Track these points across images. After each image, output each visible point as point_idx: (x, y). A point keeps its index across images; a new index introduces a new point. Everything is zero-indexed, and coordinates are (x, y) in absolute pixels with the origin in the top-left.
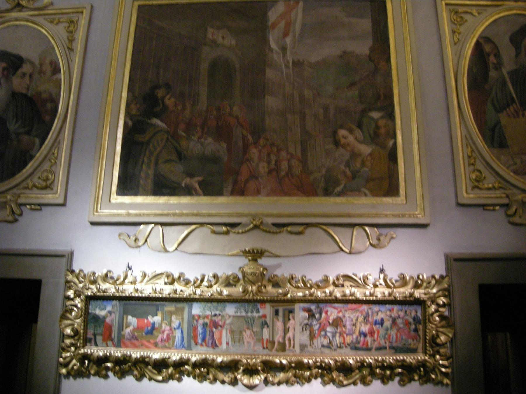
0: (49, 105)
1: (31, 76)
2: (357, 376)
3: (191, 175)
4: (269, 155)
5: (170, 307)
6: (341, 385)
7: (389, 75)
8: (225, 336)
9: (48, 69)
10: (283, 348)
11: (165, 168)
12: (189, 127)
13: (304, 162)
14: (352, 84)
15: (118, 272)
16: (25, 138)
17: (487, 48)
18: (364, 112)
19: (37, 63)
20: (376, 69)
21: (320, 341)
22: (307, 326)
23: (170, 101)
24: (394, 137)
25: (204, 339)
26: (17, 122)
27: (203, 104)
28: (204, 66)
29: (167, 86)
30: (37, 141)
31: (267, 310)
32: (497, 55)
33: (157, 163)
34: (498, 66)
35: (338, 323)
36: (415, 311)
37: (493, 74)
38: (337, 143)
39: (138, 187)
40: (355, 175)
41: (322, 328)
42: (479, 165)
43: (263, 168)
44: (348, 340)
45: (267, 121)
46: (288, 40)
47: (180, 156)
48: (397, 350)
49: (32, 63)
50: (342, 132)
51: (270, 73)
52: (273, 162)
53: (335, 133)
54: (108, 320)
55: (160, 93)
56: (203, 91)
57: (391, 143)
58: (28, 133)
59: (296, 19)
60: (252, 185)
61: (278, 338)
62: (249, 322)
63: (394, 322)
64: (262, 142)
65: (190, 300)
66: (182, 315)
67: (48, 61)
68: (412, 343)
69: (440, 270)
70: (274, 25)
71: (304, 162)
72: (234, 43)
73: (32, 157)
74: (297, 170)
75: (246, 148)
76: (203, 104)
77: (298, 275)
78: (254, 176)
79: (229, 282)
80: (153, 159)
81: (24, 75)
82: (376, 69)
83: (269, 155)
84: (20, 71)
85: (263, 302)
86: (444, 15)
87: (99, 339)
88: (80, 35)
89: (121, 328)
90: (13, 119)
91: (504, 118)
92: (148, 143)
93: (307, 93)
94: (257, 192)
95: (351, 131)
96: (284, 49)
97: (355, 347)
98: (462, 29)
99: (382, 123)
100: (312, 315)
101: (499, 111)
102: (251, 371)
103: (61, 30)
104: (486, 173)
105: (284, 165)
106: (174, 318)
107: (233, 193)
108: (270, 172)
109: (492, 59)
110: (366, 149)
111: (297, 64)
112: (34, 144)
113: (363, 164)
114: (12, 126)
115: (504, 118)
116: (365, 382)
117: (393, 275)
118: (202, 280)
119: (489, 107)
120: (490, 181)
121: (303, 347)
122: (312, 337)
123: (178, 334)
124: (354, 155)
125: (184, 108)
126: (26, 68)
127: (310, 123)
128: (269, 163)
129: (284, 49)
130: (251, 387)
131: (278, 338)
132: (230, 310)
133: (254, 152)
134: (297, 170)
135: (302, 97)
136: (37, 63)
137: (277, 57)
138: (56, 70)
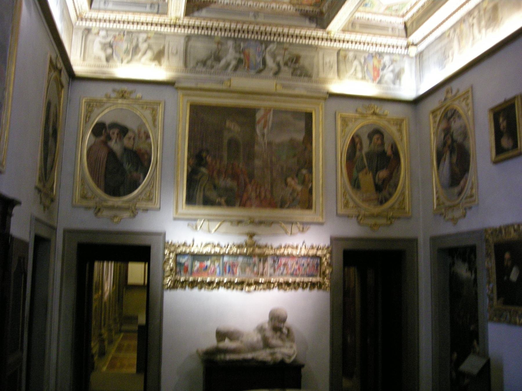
0: (146, 157)
1: (134, 139)
2: (292, 286)
3: (220, 196)
4: (256, 189)
5: (214, 258)
6: (285, 290)
7: (311, 151)
8: (238, 271)
9: (142, 135)
10: (262, 275)
11: (208, 193)
12: (219, 173)
13: (272, 192)
14: (294, 156)
15: (189, 242)
16: (135, 174)
17: (357, 140)
18: (299, 170)
19: (136, 131)
20: (305, 149)
21: (277, 273)
22: (273, 266)
23: (209, 159)
24: (312, 182)
25: (229, 271)
26: (129, 164)
27: (225, 161)
28: (225, 142)
29: (208, 151)
30: (142, 176)
31: (256, 259)
32: (361, 144)
33: (204, 190)
34: (361, 149)
35: (285, 265)
36: (316, 261)
37: (358, 153)
38: (286, 184)
39: (196, 202)
40: (294, 200)
41: (279, 267)
42: (348, 197)
43: (253, 195)
44: (289, 272)
45: (255, 171)
46: (266, 131)
47: (215, 187)
48: (309, 276)
49: (134, 132)
50: (289, 180)
51: (256, 148)
52: (258, 193)
53: (286, 180)
54: (186, 264)
55: (204, 154)
56: (225, 155)
57: (310, 186)
58: (137, 170)
59: (269, 119)
60: (248, 203)
61: (261, 270)
62: (249, 265)
63: (308, 265)
64: (253, 182)
65: (223, 255)
66: (220, 262)
67: (142, 131)
68: (315, 273)
69: (327, 243)
70: (259, 122)
71: (272, 192)
72: (239, 130)
73: (139, 185)
74: (269, 196)
75: (246, 185)
76: (225, 161)
77: (269, 244)
78: (249, 198)
79: (239, 247)
80: (202, 189)
81: (130, 138)
82: (305, 149)
83: (256, 189)
84: (127, 136)
85: (254, 256)
86: (339, 122)
87: (182, 273)
88: (160, 117)
89: (192, 267)
90: (126, 164)
91: (361, 175)
92: (199, 181)
93: (274, 159)
94: (251, 206)
95: (293, 179)
96: (263, 135)
97: (292, 275)
98: (347, 130)
99: (307, 175)
100: (274, 261)
101: (359, 171)
102: (249, 285)
103: (147, 113)
104: (350, 200)
105: (263, 194)
106: (216, 262)
107: (240, 205)
108: (257, 197)
109: (358, 146)
110: (299, 188)
111: (270, 144)
112: (140, 178)
113: (298, 195)
114: (127, 167)
115: (361, 175)
116: (295, 288)
117: (308, 244)
118: (228, 245)
119: (355, 170)
120: (351, 204)
121: (271, 275)
122: (275, 270)
123: (218, 270)
124: (294, 190)
125: (216, 163)
126: (130, 134)
127: (275, 174)
128: (256, 192)
129: (263, 135)
130: (249, 292)
131: (261, 270)
132: (240, 259)
133: (249, 187)
134: (269, 196)
135: (271, 161)
136: (136, 131)
137: (260, 139)
138: (148, 137)
